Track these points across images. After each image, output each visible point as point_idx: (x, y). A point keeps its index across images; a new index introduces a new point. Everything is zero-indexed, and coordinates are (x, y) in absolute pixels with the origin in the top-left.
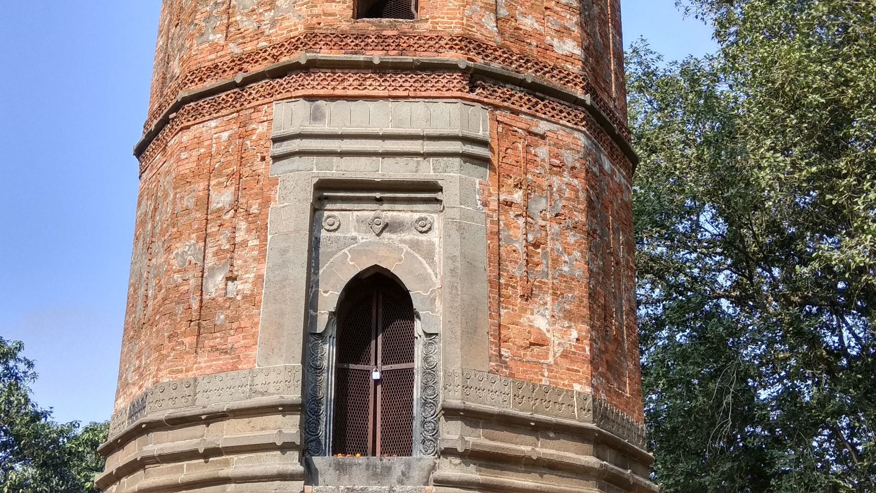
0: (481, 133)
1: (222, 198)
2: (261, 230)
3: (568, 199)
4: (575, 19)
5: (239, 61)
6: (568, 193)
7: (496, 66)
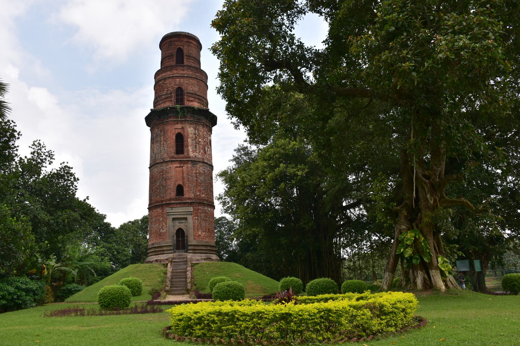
0: (192, 210)
1: (161, 219)
2: (166, 224)
5: (162, 201)
7: (194, 201)
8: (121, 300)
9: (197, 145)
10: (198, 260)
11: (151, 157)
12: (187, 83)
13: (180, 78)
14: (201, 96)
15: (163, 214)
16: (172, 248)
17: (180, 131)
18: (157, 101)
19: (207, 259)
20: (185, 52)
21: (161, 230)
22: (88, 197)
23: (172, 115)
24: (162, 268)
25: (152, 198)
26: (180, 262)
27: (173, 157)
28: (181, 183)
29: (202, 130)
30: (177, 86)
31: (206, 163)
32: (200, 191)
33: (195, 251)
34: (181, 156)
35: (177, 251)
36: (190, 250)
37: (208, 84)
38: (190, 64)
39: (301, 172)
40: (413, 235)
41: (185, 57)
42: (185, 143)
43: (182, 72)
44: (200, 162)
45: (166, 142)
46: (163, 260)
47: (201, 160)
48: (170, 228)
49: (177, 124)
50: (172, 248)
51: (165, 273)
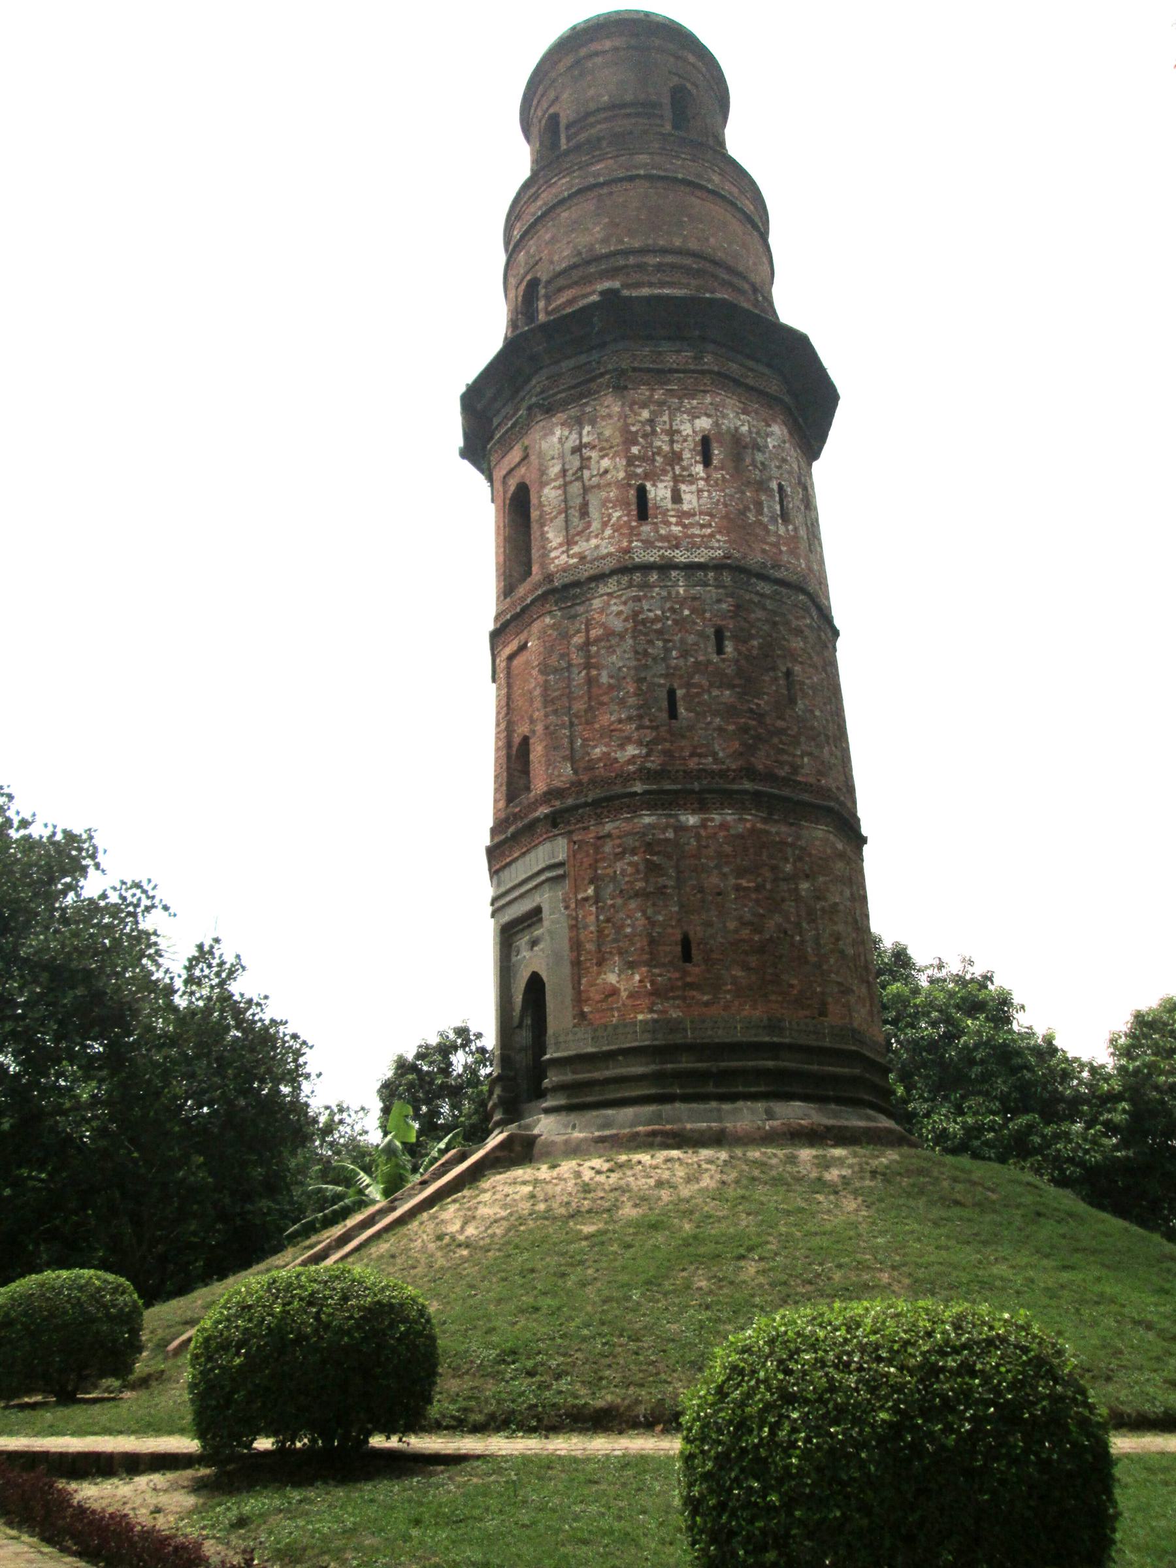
0: (561, 857)
3: (630, 875)
4: (634, 726)
6: (630, 870)
7: (570, 801)
30: (525, 283)
31: (646, 568)
32: (608, 733)
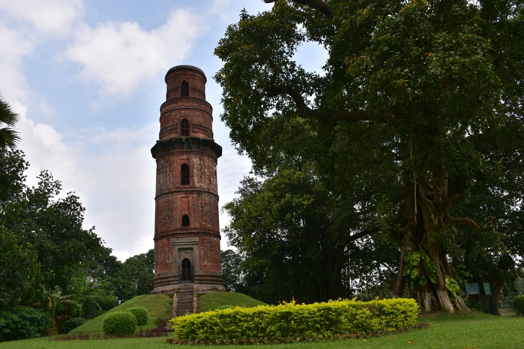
0: (198, 240)
1: (167, 250)
2: (172, 254)
5: (168, 232)
7: (199, 231)
8: (127, 326)
9: (203, 175)
10: (204, 291)
11: (157, 188)
12: (192, 115)
13: (186, 110)
14: (206, 128)
15: (169, 244)
16: (177, 279)
17: (185, 161)
18: (163, 133)
19: (213, 289)
20: (190, 85)
21: (167, 261)
22: (94, 227)
23: (177, 146)
24: (168, 298)
25: (158, 229)
26: (186, 292)
27: (178, 188)
28: (187, 213)
29: (207, 161)
30: (183, 118)
31: (211, 193)
32: (206, 221)
33: (201, 282)
34: (187, 186)
35: (183, 281)
36: (196, 280)
37: (213, 116)
38: (195, 96)
39: (307, 202)
40: (419, 256)
41: (190, 90)
42: (191, 173)
43: (187, 104)
44: (205, 192)
45: (172, 172)
46: (169, 291)
47: (206, 190)
48: (176, 258)
49: (183, 155)
50: (177, 279)
51: (171, 304)
